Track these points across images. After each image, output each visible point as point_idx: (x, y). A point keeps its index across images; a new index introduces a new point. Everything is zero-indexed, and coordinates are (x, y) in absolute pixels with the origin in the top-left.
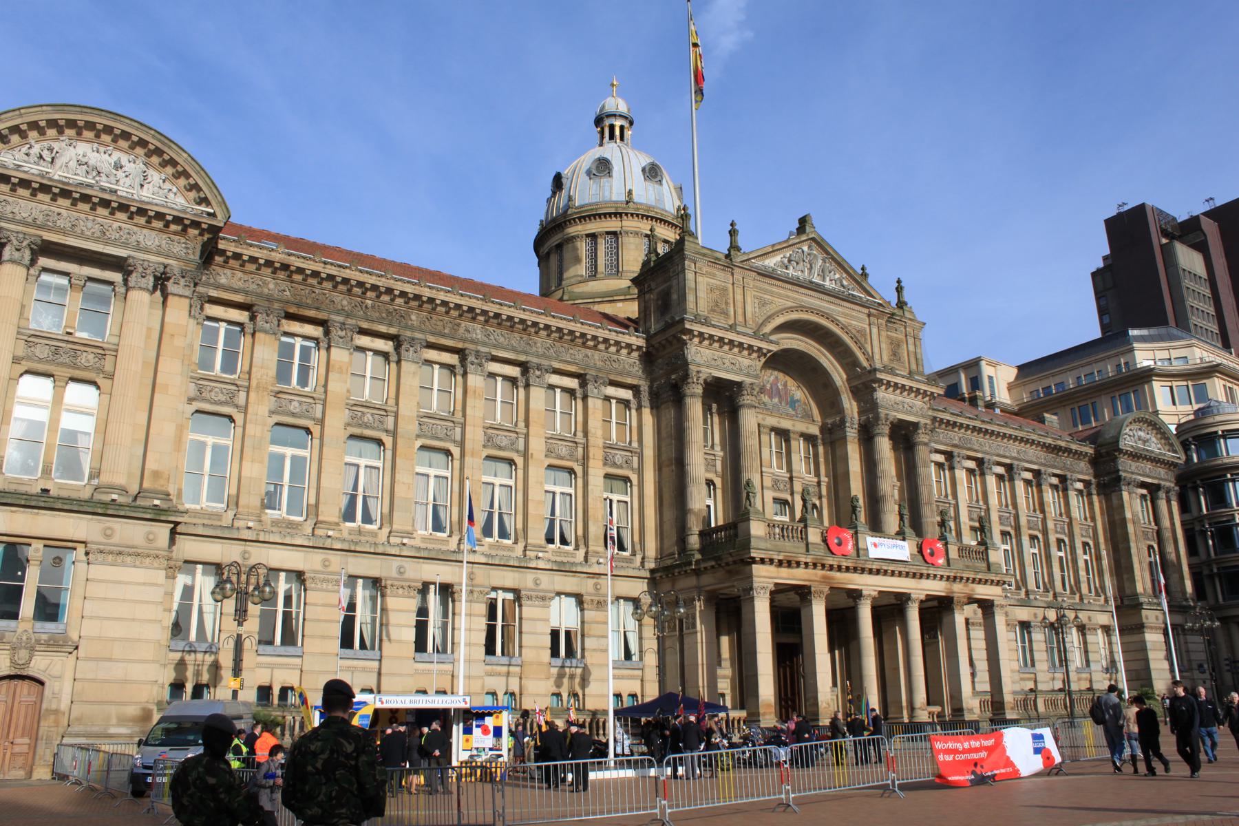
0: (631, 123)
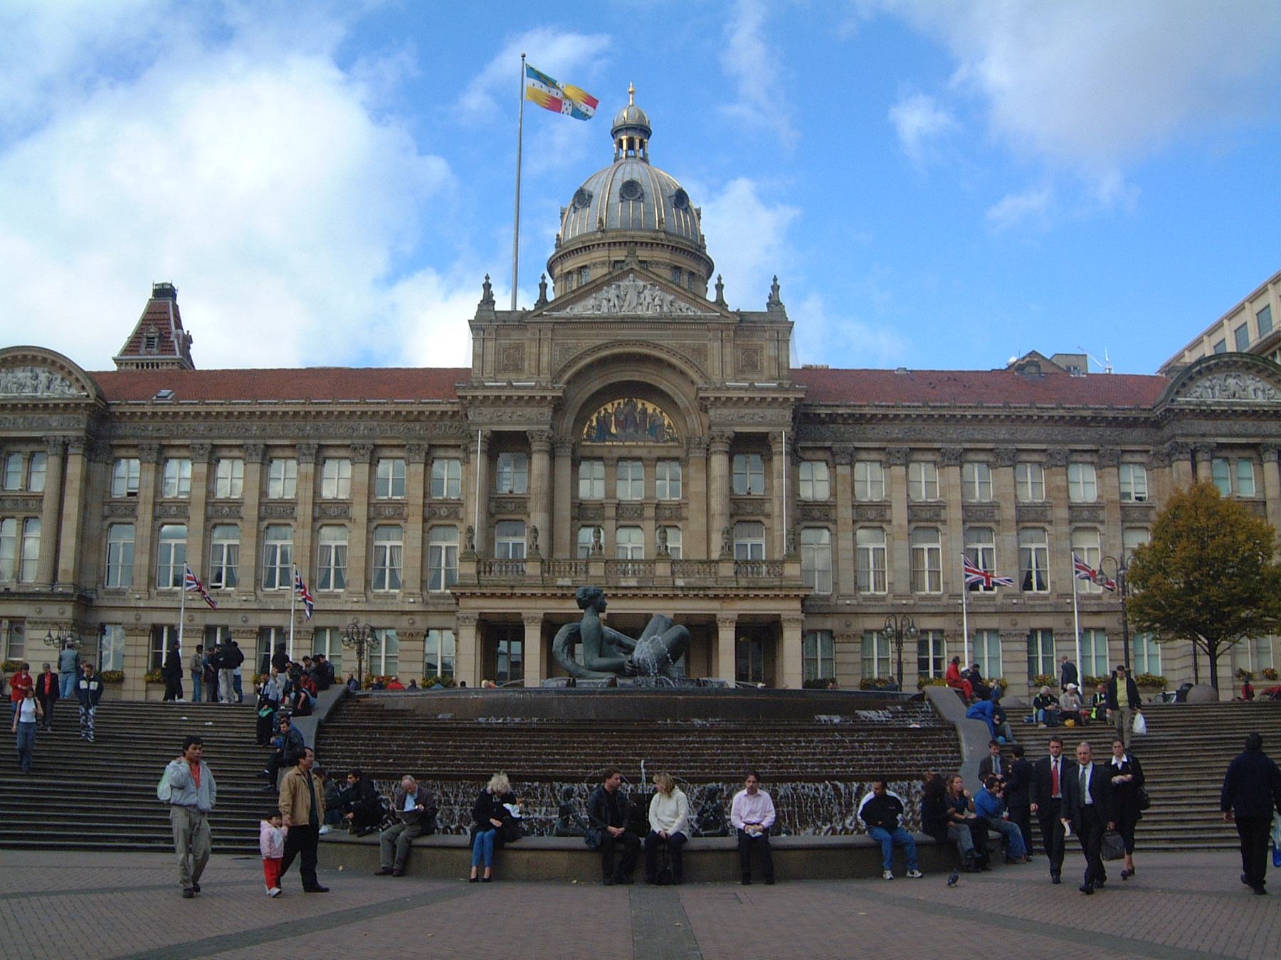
0: (645, 131)
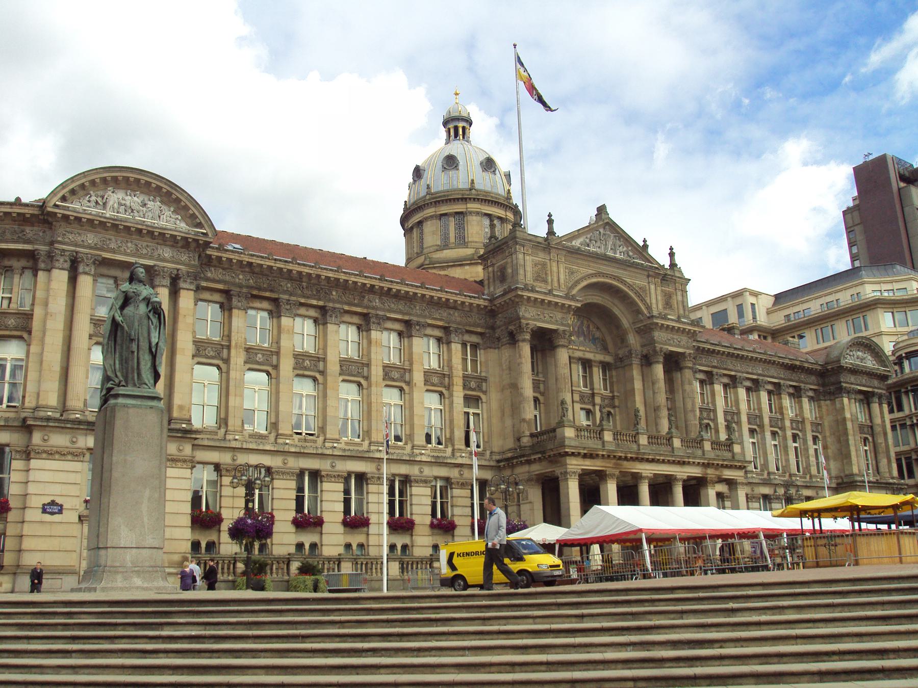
0: (471, 124)
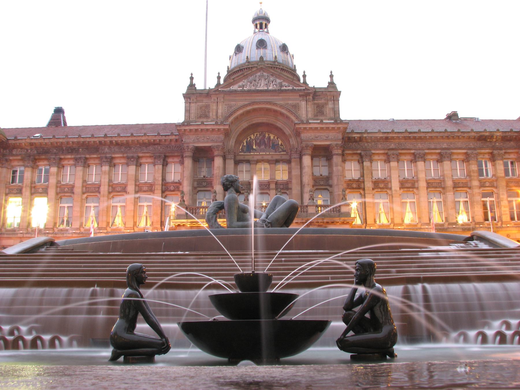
0: (268, 20)
